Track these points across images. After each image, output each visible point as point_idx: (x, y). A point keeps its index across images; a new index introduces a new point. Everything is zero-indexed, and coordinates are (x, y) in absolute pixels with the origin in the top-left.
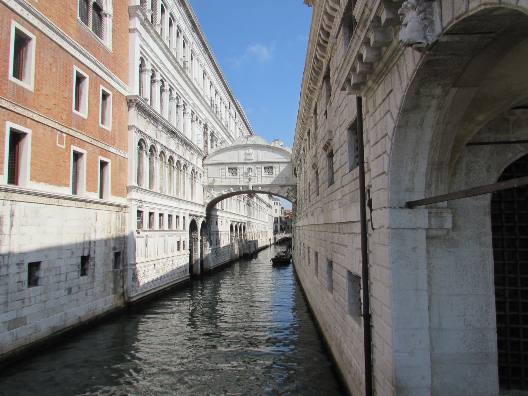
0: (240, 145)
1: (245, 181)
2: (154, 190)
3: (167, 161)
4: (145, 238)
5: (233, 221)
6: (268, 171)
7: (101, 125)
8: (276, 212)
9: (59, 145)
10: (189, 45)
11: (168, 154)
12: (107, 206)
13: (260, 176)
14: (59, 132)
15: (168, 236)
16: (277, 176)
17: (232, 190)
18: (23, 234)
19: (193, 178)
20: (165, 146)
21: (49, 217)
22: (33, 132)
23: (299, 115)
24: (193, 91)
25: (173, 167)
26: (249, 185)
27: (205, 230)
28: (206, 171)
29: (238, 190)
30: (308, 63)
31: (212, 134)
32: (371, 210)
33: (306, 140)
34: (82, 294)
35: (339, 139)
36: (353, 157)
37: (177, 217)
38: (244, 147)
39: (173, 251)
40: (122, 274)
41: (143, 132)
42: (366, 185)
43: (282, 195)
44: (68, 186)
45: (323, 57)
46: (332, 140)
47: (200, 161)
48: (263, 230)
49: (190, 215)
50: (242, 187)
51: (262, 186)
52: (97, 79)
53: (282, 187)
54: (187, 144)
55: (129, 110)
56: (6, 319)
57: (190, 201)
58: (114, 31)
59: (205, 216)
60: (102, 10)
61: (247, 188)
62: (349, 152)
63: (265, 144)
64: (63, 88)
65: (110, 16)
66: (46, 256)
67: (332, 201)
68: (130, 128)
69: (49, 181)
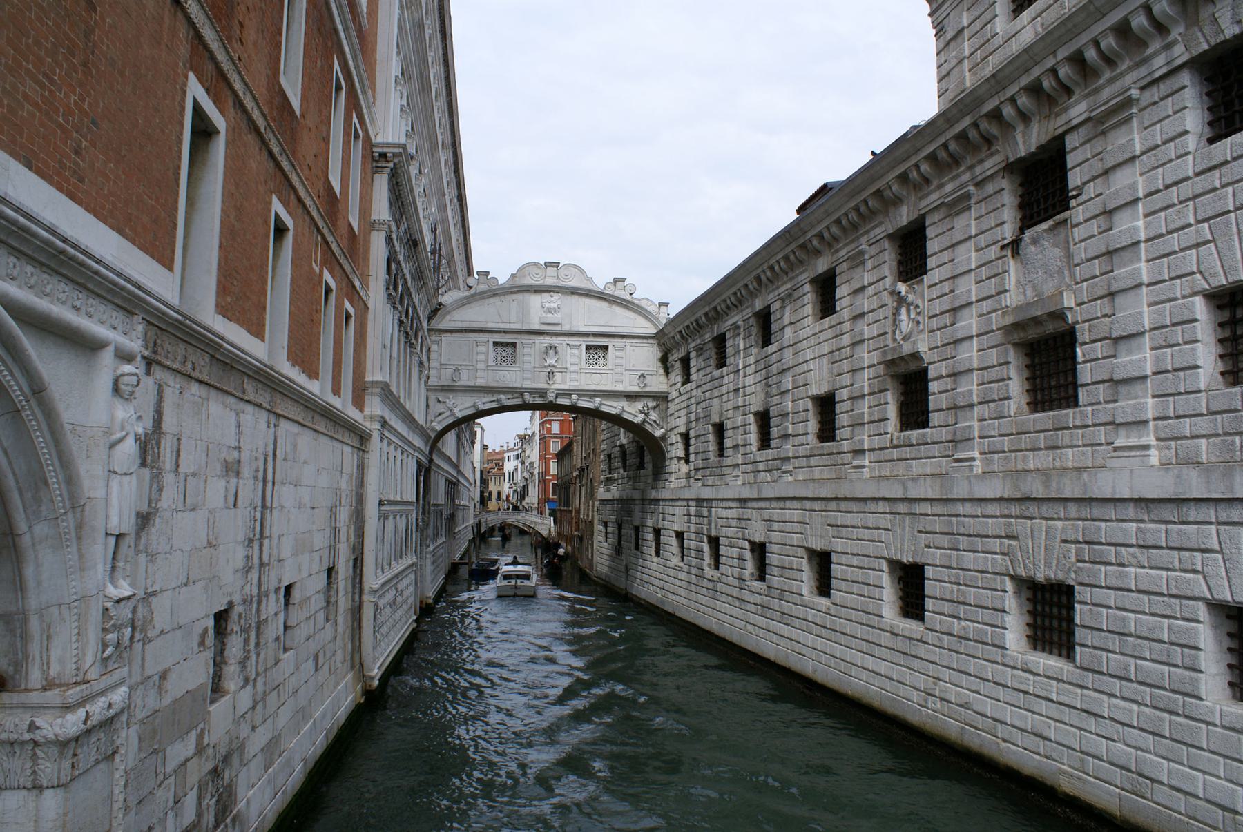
0: (528, 286)
3: (403, 318)
4: (382, 521)
6: (596, 357)
12: (352, 435)
17: (506, 400)
18: (283, 507)
19: (421, 364)
20: (405, 279)
21: (305, 462)
25: (407, 333)
26: (548, 390)
28: (434, 347)
29: (518, 401)
30: (941, 121)
34: (326, 668)
36: (1213, 357)
38: (536, 292)
50: (531, 393)
51: (582, 393)
53: (631, 397)
54: (419, 276)
56: (264, 742)
66: (300, 570)
67: (1058, 448)
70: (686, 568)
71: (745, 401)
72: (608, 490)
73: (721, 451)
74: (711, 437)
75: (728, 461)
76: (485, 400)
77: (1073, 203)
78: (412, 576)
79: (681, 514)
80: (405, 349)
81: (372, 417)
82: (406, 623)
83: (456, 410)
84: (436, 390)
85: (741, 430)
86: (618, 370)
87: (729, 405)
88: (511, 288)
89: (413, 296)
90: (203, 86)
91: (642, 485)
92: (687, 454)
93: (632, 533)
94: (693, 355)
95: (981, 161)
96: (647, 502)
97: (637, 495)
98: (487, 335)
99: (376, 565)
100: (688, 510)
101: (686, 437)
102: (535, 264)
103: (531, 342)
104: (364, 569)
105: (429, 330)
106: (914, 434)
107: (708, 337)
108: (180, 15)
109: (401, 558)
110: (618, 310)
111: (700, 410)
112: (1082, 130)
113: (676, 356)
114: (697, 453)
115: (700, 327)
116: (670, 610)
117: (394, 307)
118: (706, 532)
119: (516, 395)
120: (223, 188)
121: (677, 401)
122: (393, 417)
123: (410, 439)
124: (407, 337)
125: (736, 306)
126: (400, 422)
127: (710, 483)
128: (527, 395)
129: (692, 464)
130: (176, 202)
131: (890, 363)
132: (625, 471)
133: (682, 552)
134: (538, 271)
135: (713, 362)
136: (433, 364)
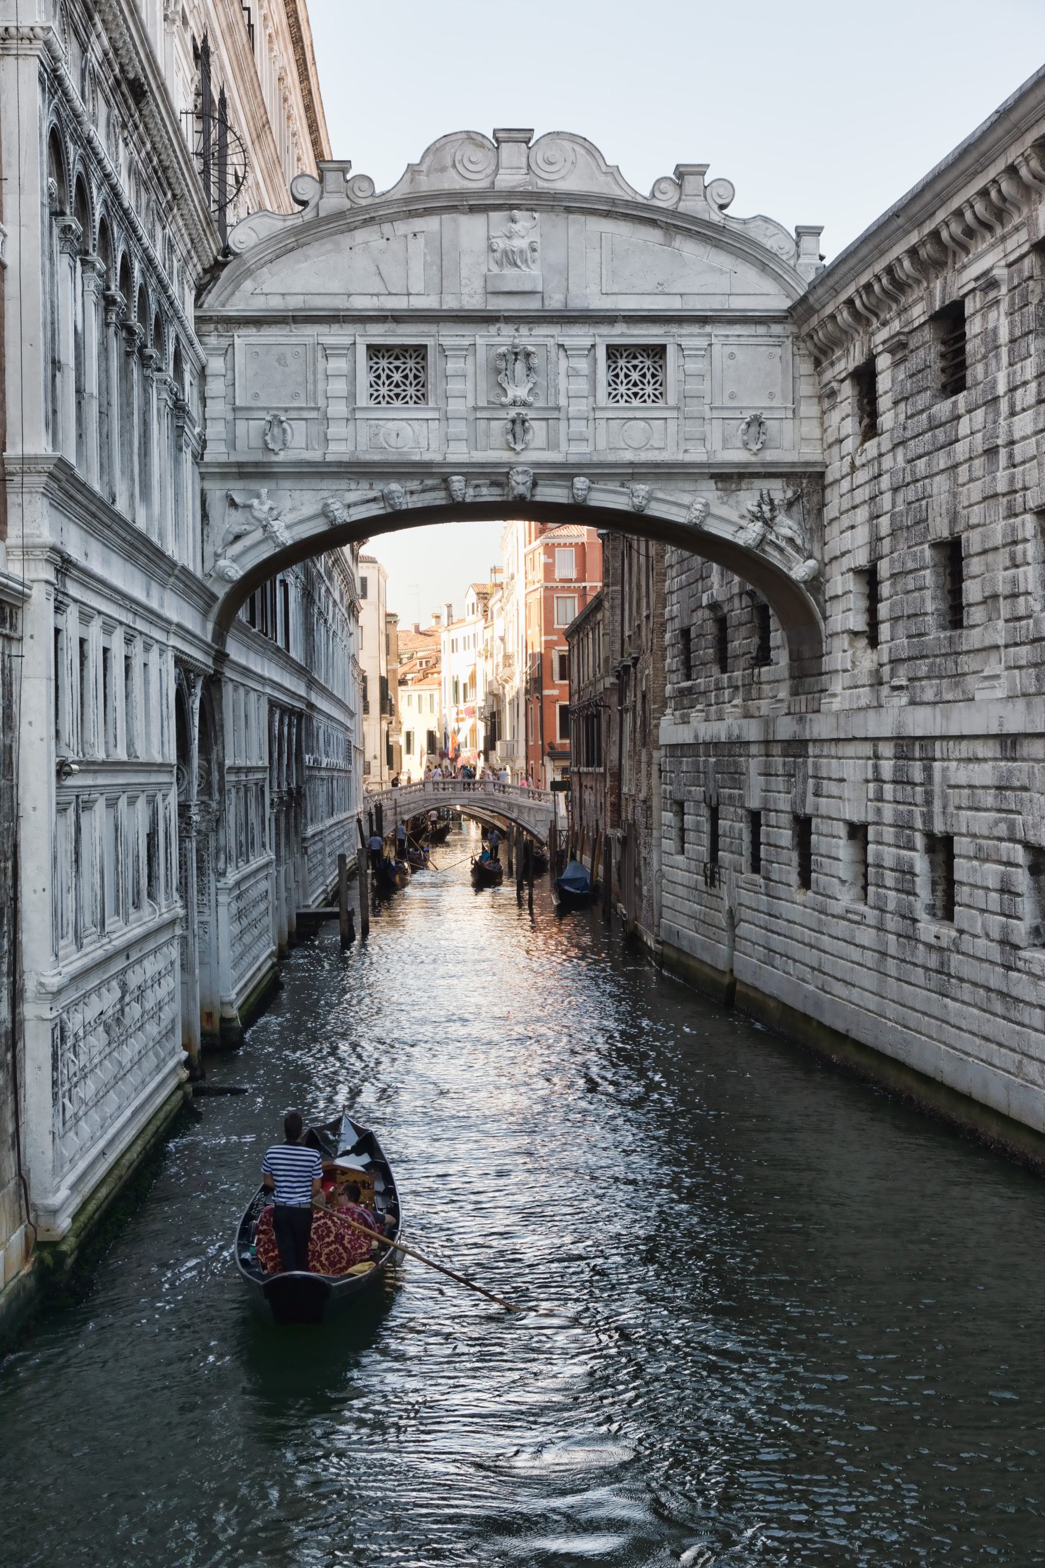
3: (115, 290)
4: (71, 812)
6: (635, 376)
19: (179, 409)
20: (113, 188)
25: (130, 331)
26: (511, 466)
28: (216, 365)
29: (437, 498)
38: (473, 209)
40: (9, 1056)
41: (60, 85)
43: (724, 532)
47: (190, 297)
48: (341, 763)
59: (210, 662)
61: (494, 484)
70: (872, 915)
71: (1012, 479)
72: (685, 721)
74: (928, 577)
75: (973, 638)
76: (352, 497)
78: (174, 952)
79: (860, 777)
80: (125, 373)
81: (26, 550)
82: (158, 1068)
83: (277, 526)
84: (224, 476)
85: (1002, 558)
86: (693, 408)
87: (975, 492)
88: (406, 201)
89: (143, 231)
91: (764, 706)
92: (874, 623)
93: (743, 828)
94: (883, 362)
96: (777, 749)
97: (752, 731)
98: (350, 329)
99: (55, 926)
100: (876, 767)
101: (869, 576)
102: (471, 138)
103: (466, 342)
104: (25, 937)
105: (199, 320)
107: (918, 313)
109: (137, 906)
110: (689, 249)
111: (900, 507)
114: (895, 620)
115: (900, 286)
116: (840, 1026)
117: (84, 262)
118: (919, 824)
119: (429, 482)
121: (845, 485)
122: (95, 547)
123: (154, 605)
124: (130, 340)
125: (989, 228)
126: (116, 561)
127: (929, 695)
128: (457, 483)
129: (884, 648)
132: (724, 670)
133: (865, 875)
134: (477, 155)
136: (215, 408)
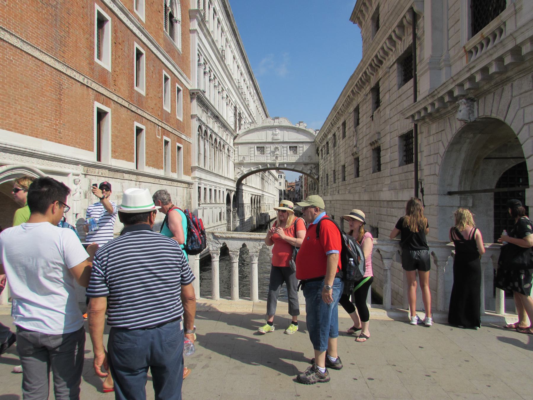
1: (272, 159)
2: (206, 169)
5: (252, 195)
7: (178, 117)
8: (280, 185)
9: (157, 136)
10: (224, 34)
11: (214, 137)
13: (285, 155)
14: (157, 126)
15: (215, 208)
16: (301, 155)
20: (212, 130)
22: (147, 128)
23: (335, 107)
24: (227, 77)
25: (217, 147)
26: (276, 163)
27: (235, 203)
28: (236, 150)
29: (266, 167)
30: (356, 74)
31: (240, 114)
32: (423, 195)
33: (338, 128)
35: (390, 142)
37: (219, 191)
38: (271, 128)
39: (217, 221)
42: (419, 178)
43: (305, 172)
44: (162, 168)
45: (373, 75)
46: (380, 139)
47: (232, 140)
48: (272, 203)
49: (227, 190)
51: (287, 164)
52: (176, 79)
53: (306, 164)
54: (224, 126)
55: (191, 102)
57: (226, 176)
58: (182, 34)
60: (174, 17)
62: (399, 152)
63: (291, 125)
64: (158, 90)
65: (179, 21)
68: (193, 117)
69: (154, 165)
73: (328, 185)
75: (329, 187)
77: (381, 104)
90: (100, 103)
95: (366, 88)
101: (322, 178)
106: (357, 179)
108: (90, 89)
112: (382, 80)
113: (320, 149)
115: (324, 139)
120: (112, 126)
130: (93, 134)
131: (353, 155)
135: (326, 152)
